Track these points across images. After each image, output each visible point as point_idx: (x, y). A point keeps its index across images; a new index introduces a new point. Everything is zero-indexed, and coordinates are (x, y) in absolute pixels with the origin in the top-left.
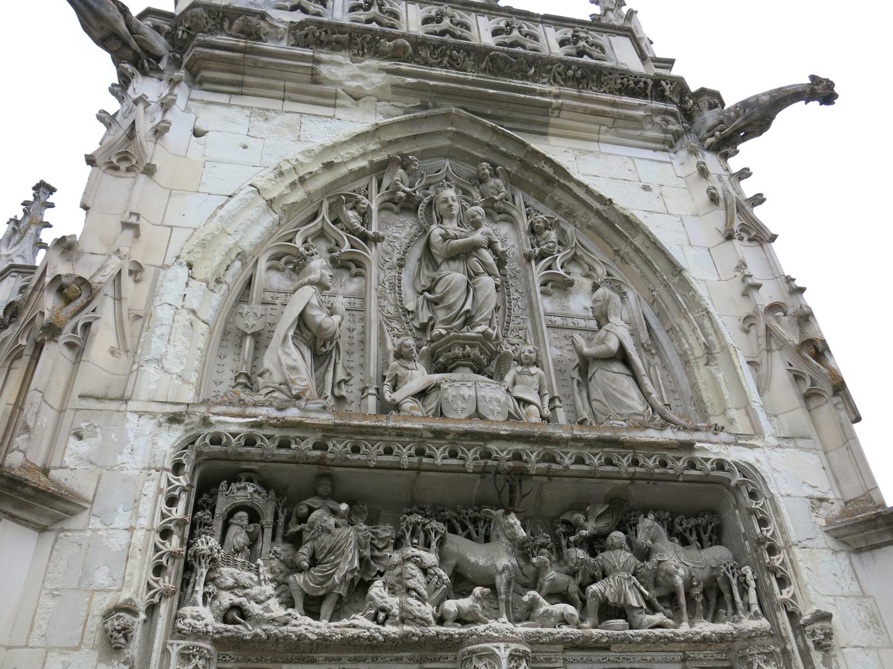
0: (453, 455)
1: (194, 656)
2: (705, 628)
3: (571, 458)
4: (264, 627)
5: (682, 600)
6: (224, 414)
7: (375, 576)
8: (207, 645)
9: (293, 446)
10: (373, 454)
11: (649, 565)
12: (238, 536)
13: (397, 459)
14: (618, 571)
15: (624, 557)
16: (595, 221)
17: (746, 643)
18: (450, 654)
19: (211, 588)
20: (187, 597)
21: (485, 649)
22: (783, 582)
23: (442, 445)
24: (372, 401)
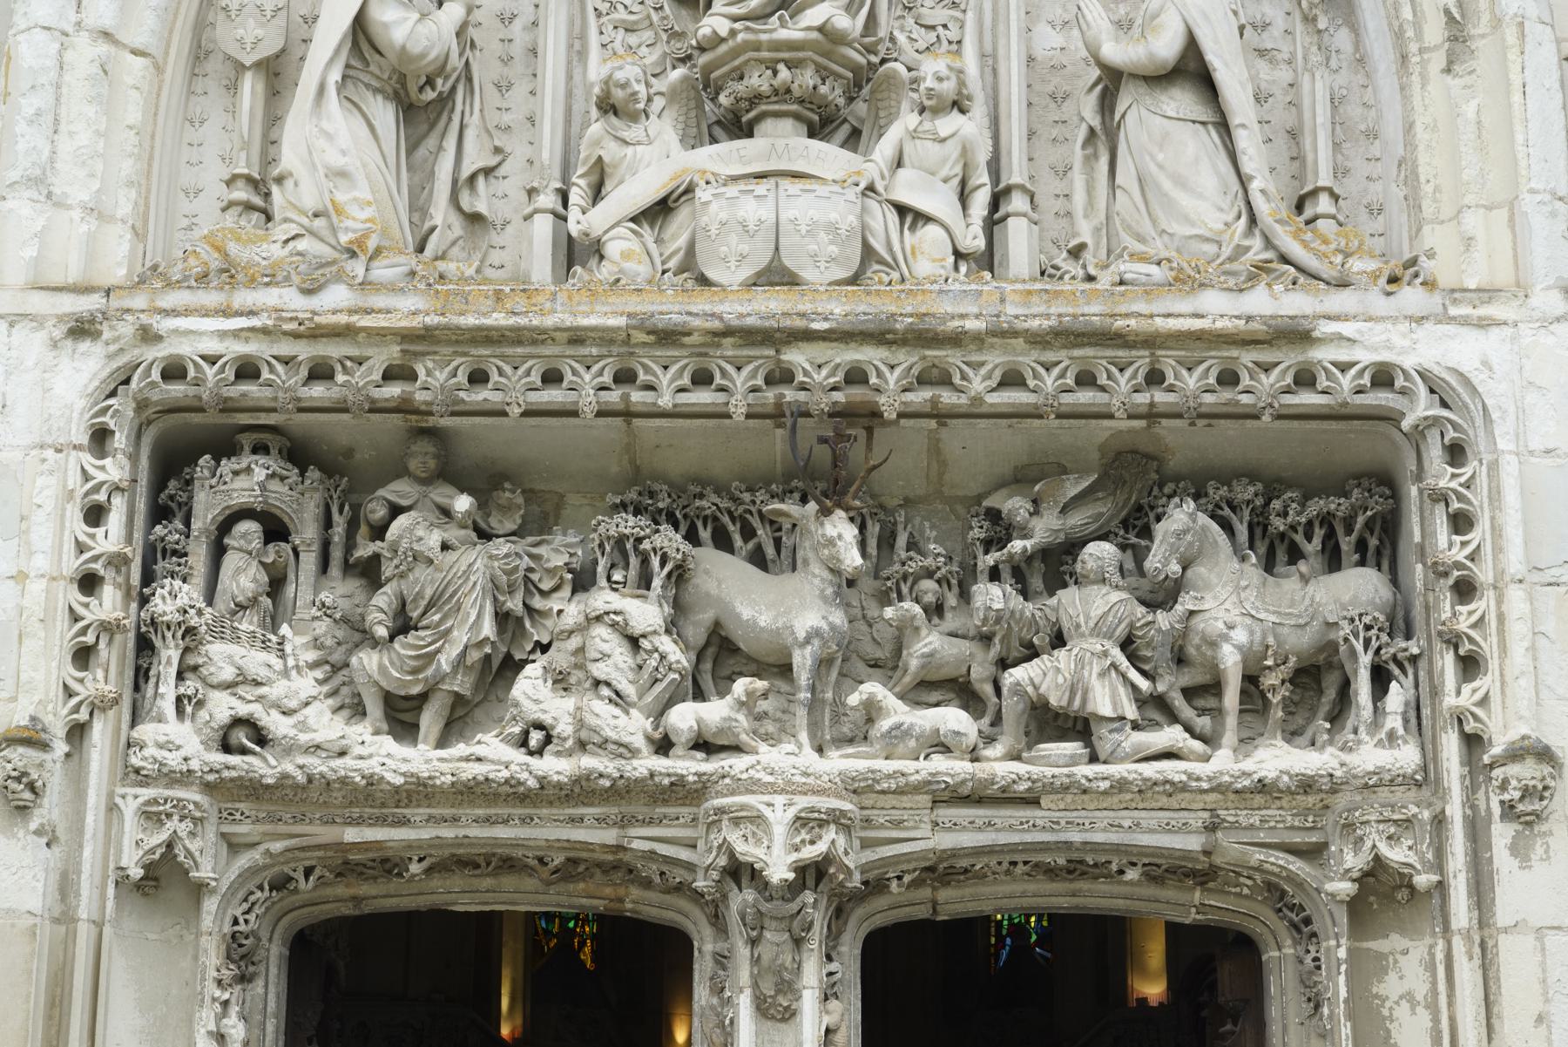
0: (702, 379)
1: (169, 816)
2: (1277, 759)
3: (989, 376)
4: (301, 760)
5: (1231, 698)
6: (187, 312)
7: (532, 651)
8: (192, 795)
9: (340, 378)
10: (514, 386)
11: (1163, 619)
12: (242, 576)
13: (572, 396)
14: (1083, 635)
17: (1358, 798)
18: (684, 810)
19: (191, 686)
20: (147, 705)
21: (743, 807)
22: (1470, 665)
23: (677, 359)
24: (543, 227)
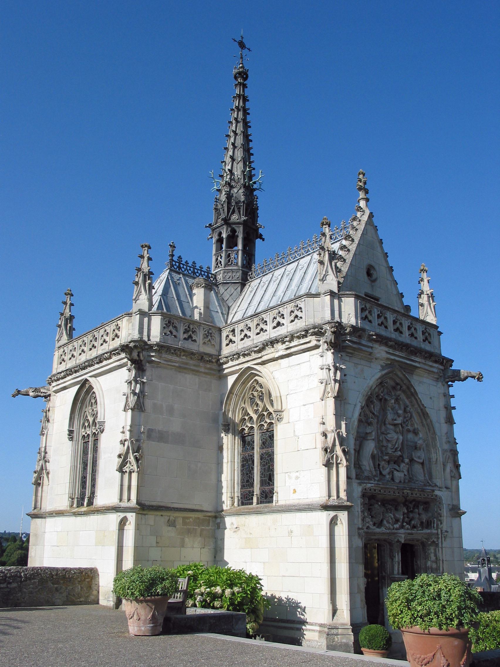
15: (418, 516)
16: (419, 411)
22: (441, 523)
